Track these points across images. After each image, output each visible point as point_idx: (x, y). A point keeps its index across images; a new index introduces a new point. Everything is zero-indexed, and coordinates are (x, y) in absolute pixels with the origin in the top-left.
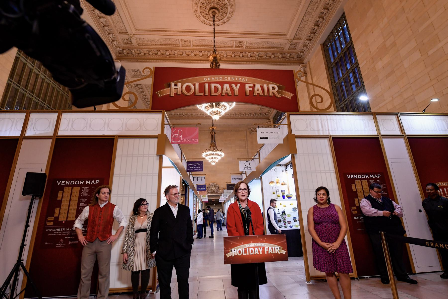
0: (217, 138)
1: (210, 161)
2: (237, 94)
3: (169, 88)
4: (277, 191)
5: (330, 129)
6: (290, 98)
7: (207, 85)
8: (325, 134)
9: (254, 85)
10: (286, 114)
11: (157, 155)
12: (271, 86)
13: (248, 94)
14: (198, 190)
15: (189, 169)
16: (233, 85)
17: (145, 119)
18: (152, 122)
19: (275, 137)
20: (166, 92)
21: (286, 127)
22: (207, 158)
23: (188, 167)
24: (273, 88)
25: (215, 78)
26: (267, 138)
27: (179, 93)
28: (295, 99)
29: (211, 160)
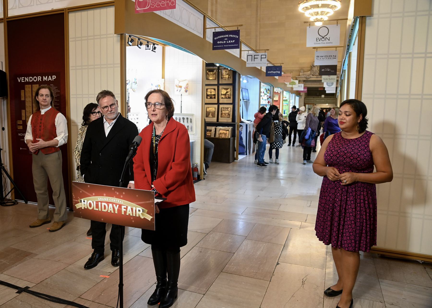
2: (116, 212)
7: (100, 203)
9: (127, 207)
13: (123, 213)
16: (114, 205)
24: (139, 210)
27: (86, 208)
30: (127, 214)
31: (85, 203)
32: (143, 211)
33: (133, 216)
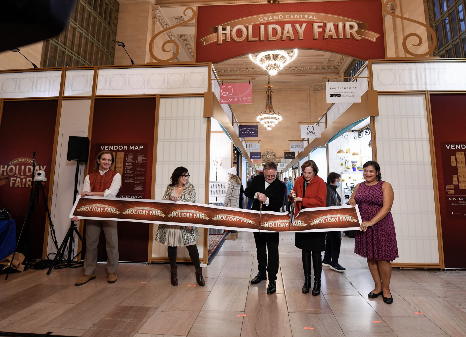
0: (274, 98)
1: (265, 125)
2: (301, 37)
3: (216, 34)
4: (347, 162)
5: (428, 82)
6: (374, 40)
7: (262, 27)
8: (420, 89)
9: (325, 24)
10: (367, 63)
11: (204, 117)
12: (348, 24)
13: (316, 37)
14: (251, 158)
15: (241, 134)
16: (297, 26)
17: (189, 74)
18: (197, 78)
19: (350, 94)
20: (212, 38)
21: (365, 81)
22: (262, 122)
23: (240, 132)
24: (351, 27)
25: (273, 18)
26: (339, 95)
27: (228, 39)
28: (381, 41)
29: (267, 124)
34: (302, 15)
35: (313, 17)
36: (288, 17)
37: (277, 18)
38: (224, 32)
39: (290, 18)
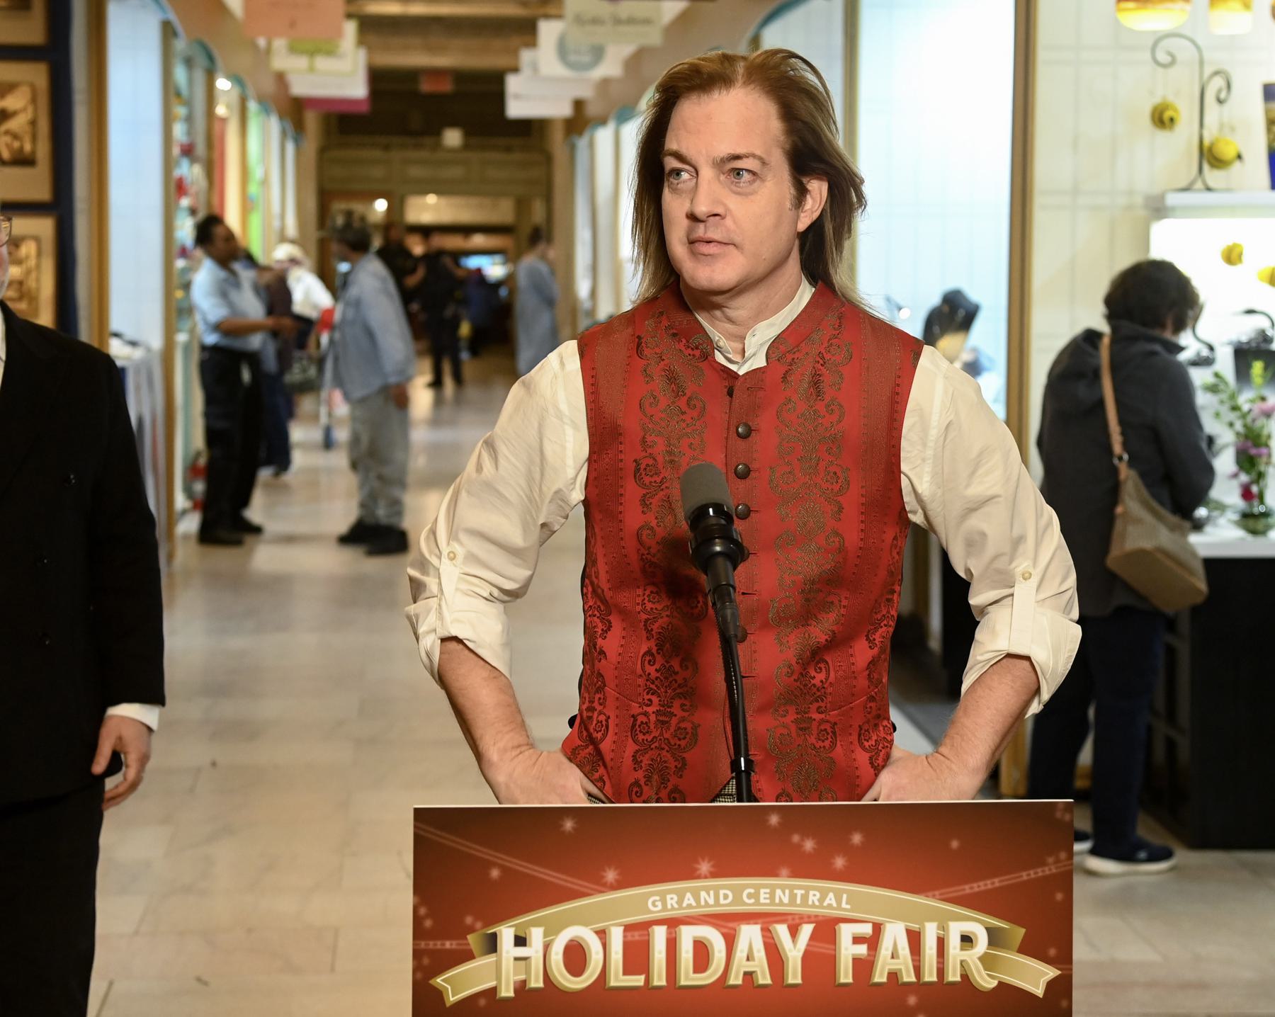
3: (492, 958)
7: (659, 935)
9: (878, 928)
16: (782, 930)
24: (967, 940)
27: (537, 982)
30: (880, 977)
31: (534, 950)
32: (995, 938)
33: (919, 986)
34: (799, 892)
35: (839, 901)
36: (749, 896)
37: (711, 901)
38: (521, 952)
39: (757, 903)
